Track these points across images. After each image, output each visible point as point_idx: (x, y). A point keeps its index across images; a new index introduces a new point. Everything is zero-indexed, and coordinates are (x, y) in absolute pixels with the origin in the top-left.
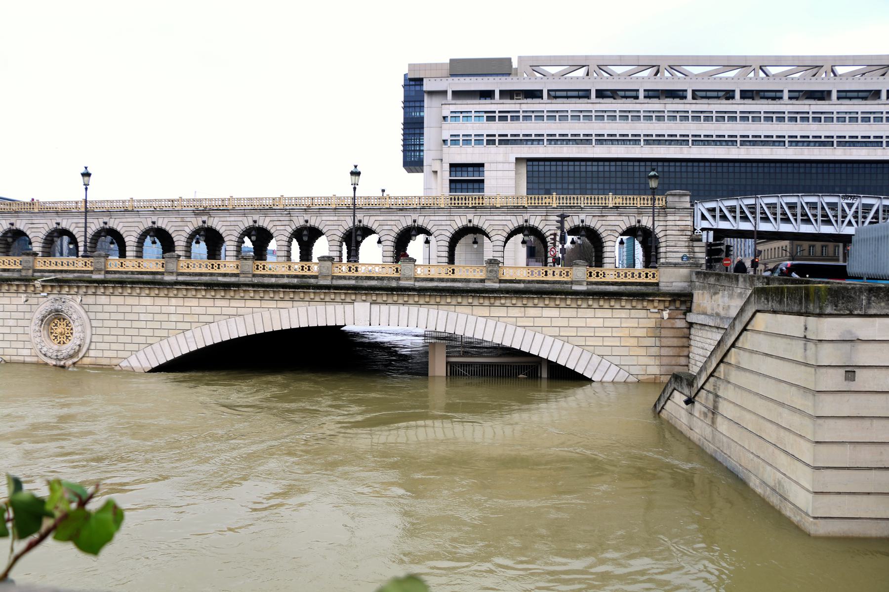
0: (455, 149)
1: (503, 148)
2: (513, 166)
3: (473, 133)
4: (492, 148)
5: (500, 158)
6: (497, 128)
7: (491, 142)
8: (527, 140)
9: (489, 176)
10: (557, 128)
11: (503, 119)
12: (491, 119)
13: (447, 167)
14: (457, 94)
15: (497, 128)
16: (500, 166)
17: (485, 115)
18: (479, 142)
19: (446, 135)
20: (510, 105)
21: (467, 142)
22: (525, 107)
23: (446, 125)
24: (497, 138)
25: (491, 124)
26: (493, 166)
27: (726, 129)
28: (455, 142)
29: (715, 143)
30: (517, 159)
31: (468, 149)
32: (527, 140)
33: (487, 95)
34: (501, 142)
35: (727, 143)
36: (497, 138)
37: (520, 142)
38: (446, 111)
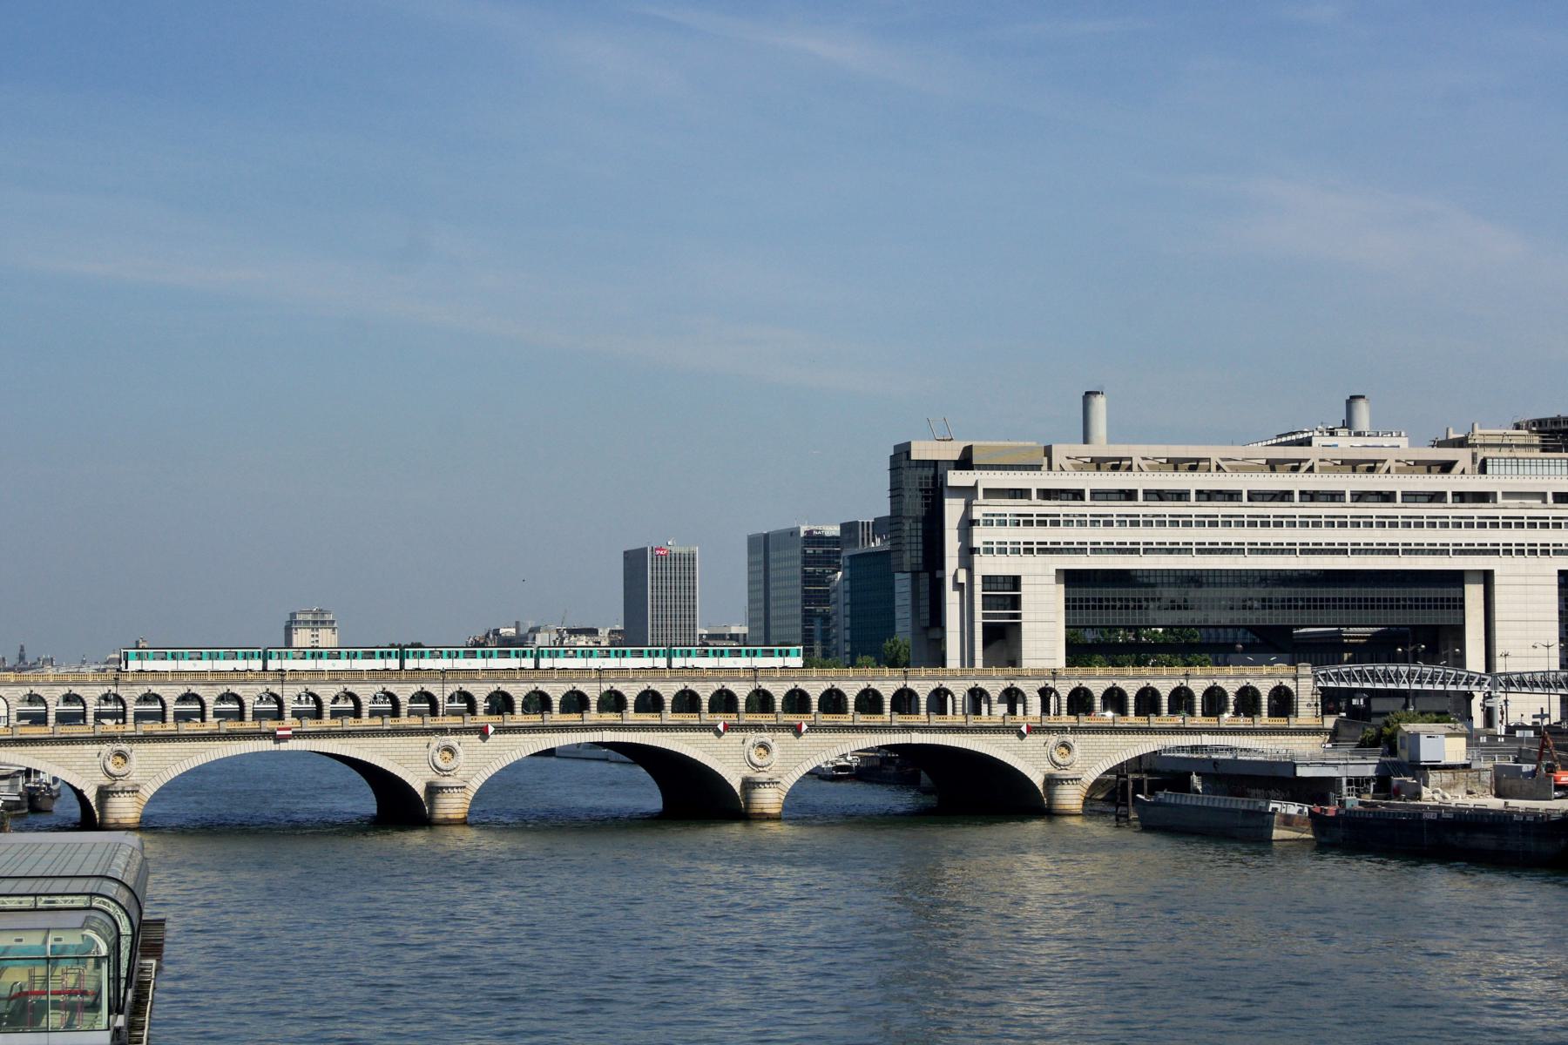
5: (1039, 570)
6: (1035, 534)
9: (1026, 592)
10: (1101, 535)
13: (978, 581)
15: (1035, 534)
16: (1039, 580)
18: (1016, 551)
20: (1051, 507)
21: (1003, 551)
24: (1035, 547)
26: (1031, 580)
27: (1284, 535)
28: (989, 551)
29: (1274, 552)
33: (1023, 493)
37: (1060, 551)
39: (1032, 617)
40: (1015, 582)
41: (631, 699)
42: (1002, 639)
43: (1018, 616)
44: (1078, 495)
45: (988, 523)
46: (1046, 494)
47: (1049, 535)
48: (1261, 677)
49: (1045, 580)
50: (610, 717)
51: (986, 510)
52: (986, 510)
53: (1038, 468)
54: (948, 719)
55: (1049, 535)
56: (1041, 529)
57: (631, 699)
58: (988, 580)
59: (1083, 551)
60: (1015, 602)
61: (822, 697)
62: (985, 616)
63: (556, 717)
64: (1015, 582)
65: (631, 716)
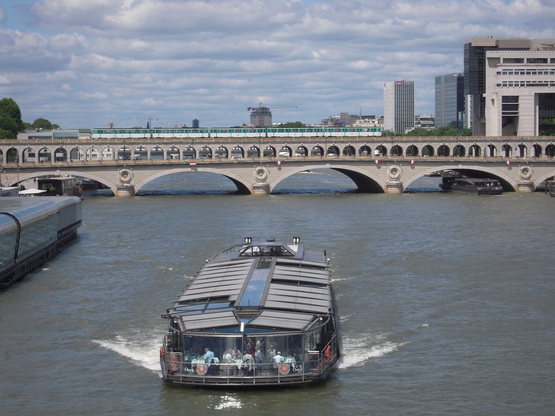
0: (505, 88)
1: (529, 88)
2: (533, 98)
3: (514, 80)
4: (523, 88)
5: (527, 93)
6: (526, 78)
7: (522, 85)
8: (540, 85)
9: (521, 102)
11: (528, 73)
12: (522, 73)
13: (501, 98)
14: (506, 60)
15: (526, 78)
17: (520, 71)
19: (500, 82)
20: (532, 66)
22: (539, 68)
23: (500, 76)
24: (525, 83)
25: (523, 76)
30: (535, 94)
31: (511, 89)
32: (540, 85)
34: (528, 85)
35: (543, 85)
36: (525, 83)
38: (500, 69)
39: (524, 114)
40: (516, 98)
41: (341, 149)
42: (510, 122)
43: (517, 113)
44: (545, 61)
45: (504, 73)
46: (530, 61)
47: (532, 78)
48: (450, 141)
49: (530, 98)
50: (348, 158)
51: (504, 68)
52: (504, 68)
53: (528, 49)
54: (481, 159)
55: (532, 78)
56: (528, 76)
57: (341, 149)
58: (505, 98)
59: (547, 85)
60: (516, 107)
61: (424, 149)
62: (503, 113)
63: (342, 157)
64: (516, 98)
65: (342, 157)
